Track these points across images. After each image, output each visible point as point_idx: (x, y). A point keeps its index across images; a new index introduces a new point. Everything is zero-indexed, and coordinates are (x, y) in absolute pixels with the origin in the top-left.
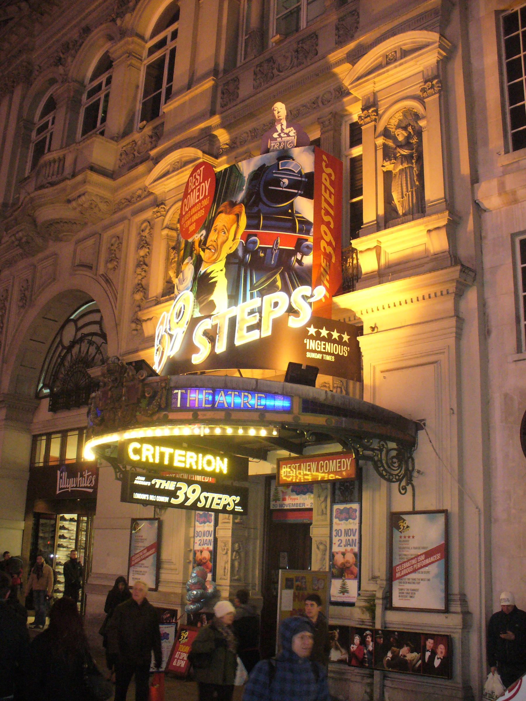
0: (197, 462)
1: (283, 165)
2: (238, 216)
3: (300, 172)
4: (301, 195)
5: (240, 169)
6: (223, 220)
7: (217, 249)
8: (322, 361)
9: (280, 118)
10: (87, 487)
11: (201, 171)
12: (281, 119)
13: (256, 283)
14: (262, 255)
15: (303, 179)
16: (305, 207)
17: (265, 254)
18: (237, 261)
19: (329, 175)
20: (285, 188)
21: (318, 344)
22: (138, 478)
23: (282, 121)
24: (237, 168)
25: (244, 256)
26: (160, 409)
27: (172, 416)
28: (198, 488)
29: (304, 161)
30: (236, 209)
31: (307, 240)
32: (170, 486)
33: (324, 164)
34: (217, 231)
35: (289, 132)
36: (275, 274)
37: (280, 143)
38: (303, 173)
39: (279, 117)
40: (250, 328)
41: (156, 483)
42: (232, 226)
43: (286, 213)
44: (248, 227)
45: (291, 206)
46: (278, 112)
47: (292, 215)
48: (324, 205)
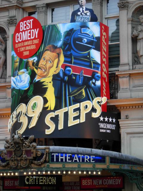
1: (84, 30)
3: (93, 36)
4: (94, 49)
5: (58, 28)
6: (48, 55)
7: (47, 70)
8: (106, 133)
9: (82, 4)
11: (30, 22)
12: (83, 6)
13: (72, 92)
14: (74, 78)
15: (95, 40)
16: (96, 55)
17: (76, 77)
19: (105, 36)
20: (85, 43)
23: (83, 6)
24: (56, 27)
25: (64, 77)
29: (94, 30)
30: (57, 51)
31: (97, 73)
33: (103, 31)
34: (45, 60)
35: (87, 13)
36: (82, 89)
37: (81, 18)
38: (94, 37)
39: (81, 4)
40: (75, 118)
42: (55, 59)
43: (86, 57)
44: (65, 61)
45: (89, 54)
46: (81, 2)
47: (89, 58)
48: (103, 53)
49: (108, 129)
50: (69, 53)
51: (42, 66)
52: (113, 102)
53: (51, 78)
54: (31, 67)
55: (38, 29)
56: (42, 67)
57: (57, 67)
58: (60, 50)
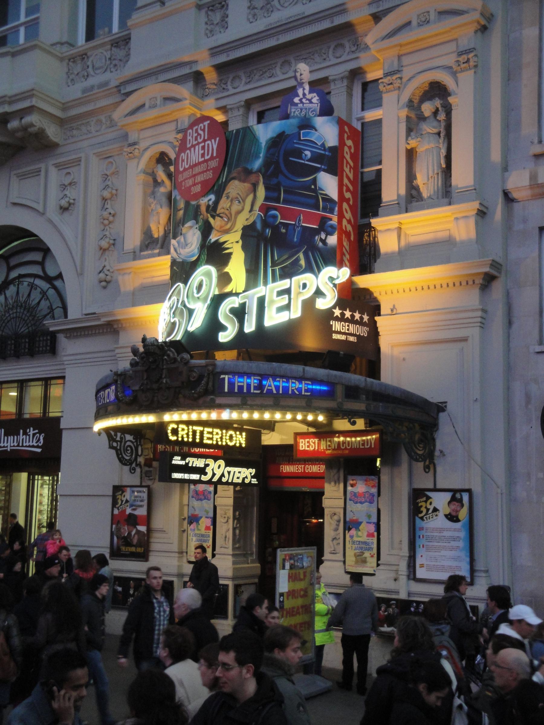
0: (221, 438)
1: (305, 135)
2: (255, 187)
3: (323, 145)
4: (324, 171)
5: (255, 133)
6: (235, 188)
7: (231, 218)
8: (346, 342)
9: (303, 81)
10: (33, 446)
11: (204, 126)
12: (303, 83)
14: (284, 231)
15: (327, 153)
16: (329, 184)
17: (286, 230)
18: (255, 234)
19: (350, 148)
20: (307, 161)
21: (343, 326)
22: (176, 458)
23: (304, 85)
24: (252, 132)
26: (206, 392)
27: (219, 400)
28: (222, 462)
29: (327, 133)
30: (253, 178)
31: (331, 220)
32: (199, 463)
33: (346, 136)
34: (230, 199)
35: (312, 98)
36: (298, 252)
37: (301, 109)
38: (327, 147)
39: (301, 80)
40: (280, 309)
41: (189, 461)
42: (247, 195)
43: (309, 189)
44: (267, 199)
45: (314, 181)
46: (301, 75)
47: (315, 191)
48: (346, 181)
49: (351, 334)
50: (274, 181)
51: (222, 211)
52: (363, 281)
53: (239, 233)
54: (203, 215)
55: (218, 139)
56: (223, 213)
57: (251, 211)
58: (259, 176)
